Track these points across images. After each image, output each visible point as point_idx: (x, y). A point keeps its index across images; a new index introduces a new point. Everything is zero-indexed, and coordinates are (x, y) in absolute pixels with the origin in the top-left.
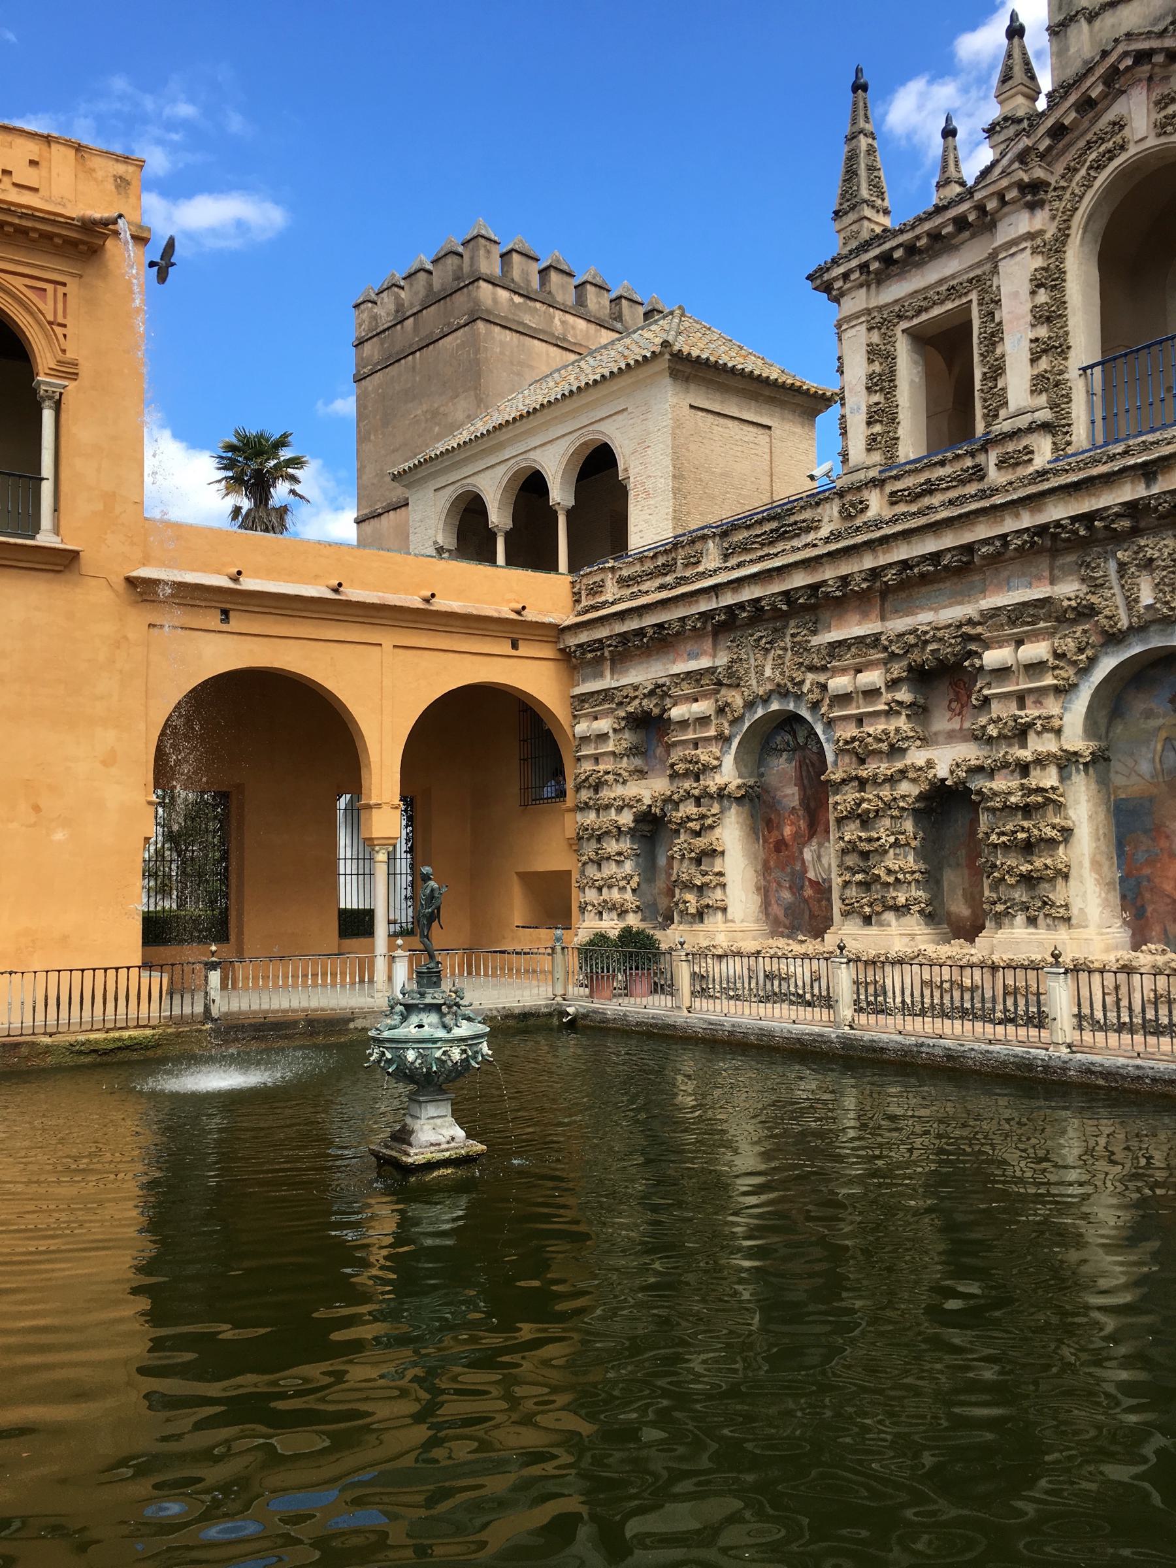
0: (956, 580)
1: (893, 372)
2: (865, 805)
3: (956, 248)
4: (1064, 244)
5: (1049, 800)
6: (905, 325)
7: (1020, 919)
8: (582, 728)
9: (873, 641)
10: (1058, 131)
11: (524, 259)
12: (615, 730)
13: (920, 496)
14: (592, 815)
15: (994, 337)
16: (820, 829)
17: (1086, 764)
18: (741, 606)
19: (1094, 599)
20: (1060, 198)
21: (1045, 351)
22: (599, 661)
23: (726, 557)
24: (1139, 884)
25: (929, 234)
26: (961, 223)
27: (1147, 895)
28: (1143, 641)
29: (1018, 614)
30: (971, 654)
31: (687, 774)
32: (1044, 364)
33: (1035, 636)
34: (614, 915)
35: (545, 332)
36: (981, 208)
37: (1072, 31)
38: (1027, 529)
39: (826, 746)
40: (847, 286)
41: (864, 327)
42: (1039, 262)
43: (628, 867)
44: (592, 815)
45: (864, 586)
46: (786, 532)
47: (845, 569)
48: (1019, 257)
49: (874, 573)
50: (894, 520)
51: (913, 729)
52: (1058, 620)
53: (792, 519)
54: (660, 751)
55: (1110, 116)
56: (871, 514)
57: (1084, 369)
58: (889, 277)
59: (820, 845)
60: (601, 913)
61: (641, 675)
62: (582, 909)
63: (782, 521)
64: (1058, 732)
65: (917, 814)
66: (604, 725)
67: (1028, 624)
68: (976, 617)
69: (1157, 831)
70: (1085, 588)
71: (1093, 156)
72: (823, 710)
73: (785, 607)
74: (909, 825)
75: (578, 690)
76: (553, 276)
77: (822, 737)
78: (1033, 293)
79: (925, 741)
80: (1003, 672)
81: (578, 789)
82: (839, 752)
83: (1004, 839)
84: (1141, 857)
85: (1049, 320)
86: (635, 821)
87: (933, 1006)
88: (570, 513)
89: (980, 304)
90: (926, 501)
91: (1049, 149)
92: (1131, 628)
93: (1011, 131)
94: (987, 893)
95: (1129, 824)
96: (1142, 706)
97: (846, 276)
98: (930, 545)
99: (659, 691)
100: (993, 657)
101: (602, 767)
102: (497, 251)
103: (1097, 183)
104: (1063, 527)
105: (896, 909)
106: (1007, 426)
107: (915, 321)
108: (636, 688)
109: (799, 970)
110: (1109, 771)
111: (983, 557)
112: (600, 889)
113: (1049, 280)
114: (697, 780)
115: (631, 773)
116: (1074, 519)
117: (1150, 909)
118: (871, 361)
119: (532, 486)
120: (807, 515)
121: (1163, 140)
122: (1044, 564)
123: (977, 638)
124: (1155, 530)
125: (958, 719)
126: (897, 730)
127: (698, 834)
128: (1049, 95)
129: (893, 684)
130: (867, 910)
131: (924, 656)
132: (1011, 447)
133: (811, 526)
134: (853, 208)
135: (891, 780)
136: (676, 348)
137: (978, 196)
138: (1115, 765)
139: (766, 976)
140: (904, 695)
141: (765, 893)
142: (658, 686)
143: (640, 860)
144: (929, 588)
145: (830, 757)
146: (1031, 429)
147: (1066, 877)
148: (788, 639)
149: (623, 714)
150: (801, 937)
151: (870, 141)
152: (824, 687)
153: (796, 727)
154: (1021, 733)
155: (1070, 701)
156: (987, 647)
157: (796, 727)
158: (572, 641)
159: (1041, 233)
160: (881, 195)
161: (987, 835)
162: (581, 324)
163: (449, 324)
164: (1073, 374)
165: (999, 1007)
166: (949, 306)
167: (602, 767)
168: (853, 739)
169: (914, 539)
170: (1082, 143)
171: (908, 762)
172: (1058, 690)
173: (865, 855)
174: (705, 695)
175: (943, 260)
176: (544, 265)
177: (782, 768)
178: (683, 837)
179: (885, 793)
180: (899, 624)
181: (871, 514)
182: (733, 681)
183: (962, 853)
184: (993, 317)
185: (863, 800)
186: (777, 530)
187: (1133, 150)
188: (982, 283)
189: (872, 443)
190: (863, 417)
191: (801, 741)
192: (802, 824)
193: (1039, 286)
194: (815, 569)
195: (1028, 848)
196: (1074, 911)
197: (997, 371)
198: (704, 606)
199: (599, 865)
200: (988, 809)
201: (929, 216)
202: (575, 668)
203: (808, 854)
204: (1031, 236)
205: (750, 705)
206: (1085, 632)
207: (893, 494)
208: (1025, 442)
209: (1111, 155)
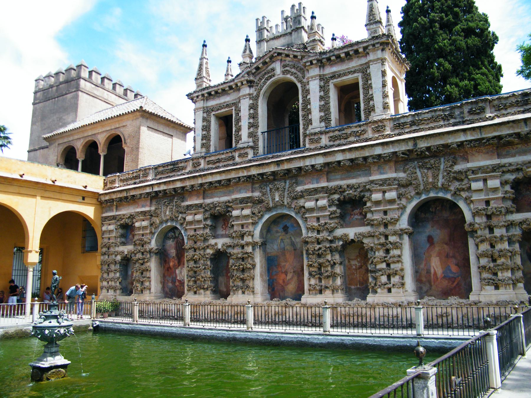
0: (225, 189)
1: (210, 126)
2: (196, 256)
3: (229, 94)
4: (258, 98)
5: (249, 256)
7: (240, 291)
8: (104, 228)
9: (200, 206)
10: (257, 68)
11: (96, 74)
12: (116, 229)
13: (216, 163)
14: (107, 257)
15: (239, 120)
16: (182, 263)
17: (260, 246)
18: (160, 191)
19: (263, 198)
20: (257, 86)
21: (252, 126)
22: (112, 206)
23: (156, 175)
24: (273, 281)
25: (222, 89)
26: (231, 88)
27: (275, 284)
28: (276, 211)
29: (243, 201)
30: (229, 211)
31: (139, 244)
32: (252, 130)
33: (247, 207)
34: (112, 291)
35: (101, 97)
36: (237, 85)
37: (262, 43)
38: (246, 176)
39: (184, 237)
41: (202, 112)
42: (251, 102)
43: (118, 275)
44: (107, 257)
45: (198, 188)
47: (192, 182)
49: (202, 185)
51: (211, 233)
52: (253, 203)
53: (177, 166)
54: (131, 236)
55: (271, 67)
56: (202, 166)
57: (262, 133)
58: (210, 99)
59: (181, 269)
60: (108, 290)
61: (126, 211)
62: (102, 288)
63: (174, 166)
64: (253, 236)
65: (212, 260)
66: (112, 227)
69: (279, 265)
70: (261, 194)
71: (266, 76)
72: (184, 226)
74: (209, 263)
75: (104, 215)
76: (106, 80)
77: (183, 235)
78: (249, 110)
79: (215, 237)
80: (237, 217)
81: (102, 248)
82: (188, 239)
83: (236, 267)
84: (274, 273)
85: (253, 118)
86: (121, 259)
87: (214, 319)
88: (105, 157)
89: (235, 110)
90: (218, 164)
91: (255, 72)
92: (272, 207)
93: (246, 66)
94: (231, 284)
95: (272, 264)
96: (275, 229)
97: (197, 97)
98: (218, 178)
99: (132, 217)
100: (235, 213)
101: (111, 241)
102: (87, 70)
103: (267, 84)
104: (255, 177)
105: (204, 289)
107: (217, 112)
108: (124, 215)
109: (173, 308)
110: (266, 248)
111: (233, 183)
112: (108, 282)
113: (254, 107)
114: (143, 246)
115: (121, 243)
116: (258, 174)
117: (276, 288)
118: (203, 122)
119: (92, 146)
120: (183, 165)
121: (284, 76)
122: (250, 185)
123: (231, 207)
124: (280, 180)
125: (224, 231)
126: (206, 233)
127: (142, 264)
128: (256, 59)
129: (206, 219)
130: (195, 289)
132: (242, 152)
133: (184, 168)
134: (201, 78)
135: (204, 249)
136: (144, 109)
137: (236, 81)
138: (268, 246)
139: (163, 311)
140: (209, 222)
141: (163, 283)
142: (131, 215)
143: (122, 272)
144: (217, 191)
145: (186, 241)
146: (247, 147)
147: (253, 279)
148: (174, 203)
149: (119, 224)
150: (174, 298)
151: (206, 60)
152: (185, 219)
153: (176, 231)
154: (242, 236)
155: (256, 227)
156: (233, 209)
157: (176, 231)
158: (103, 198)
159: (252, 94)
160: (209, 76)
161: (232, 266)
162: (114, 96)
163: (69, 91)
164: (259, 133)
165: (233, 318)
166: (227, 109)
167: (111, 241)
168: (193, 236)
169: (214, 176)
170: (263, 73)
171: (209, 243)
172: (253, 224)
173: (195, 272)
174: (147, 219)
175: (226, 96)
176: (102, 76)
177: (171, 243)
178: (137, 265)
179: (202, 252)
180: (208, 201)
181: (202, 166)
182: (156, 215)
183: (224, 272)
185: (195, 255)
186: (172, 169)
187: (276, 77)
188: (236, 104)
189: (203, 145)
191: (177, 235)
192: (176, 262)
194: (184, 182)
195: (243, 270)
196: (255, 289)
197: (239, 129)
198: (148, 190)
199: (108, 274)
200: (232, 258)
201: (222, 84)
202: (103, 207)
203: (178, 272)
204: (249, 94)
205: (161, 223)
207: (208, 161)
208: (246, 151)
209: (271, 77)
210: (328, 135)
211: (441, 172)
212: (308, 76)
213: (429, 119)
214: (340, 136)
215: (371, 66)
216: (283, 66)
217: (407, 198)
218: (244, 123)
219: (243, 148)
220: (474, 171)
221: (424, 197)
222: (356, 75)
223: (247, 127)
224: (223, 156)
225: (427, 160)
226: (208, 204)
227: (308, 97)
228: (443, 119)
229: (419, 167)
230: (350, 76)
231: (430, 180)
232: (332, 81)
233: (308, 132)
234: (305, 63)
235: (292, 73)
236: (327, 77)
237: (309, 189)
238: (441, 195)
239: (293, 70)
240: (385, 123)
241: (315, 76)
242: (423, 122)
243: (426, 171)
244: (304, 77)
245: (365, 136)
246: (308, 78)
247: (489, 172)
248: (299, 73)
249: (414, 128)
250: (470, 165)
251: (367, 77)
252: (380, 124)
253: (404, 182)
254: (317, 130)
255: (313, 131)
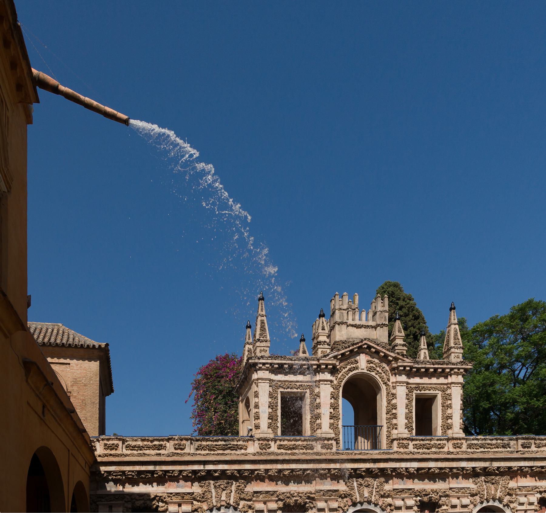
6: (282, 390)
18: (215, 471)
32: (332, 421)
40: (263, 367)
42: (332, 390)
46: (232, 447)
48: (327, 386)
50: (282, 454)
67: (330, 496)
68: (313, 492)
70: (347, 489)
71: (349, 367)
73: (238, 475)
78: (331, 399)
85: (334, 409)
89: (311, 394)
92: (360, 502)
106: (324, 436)
107: (286, 390)
113: (334, 396)
123: (313, 499)
131: (292, 501)
164: (340, 426)
184: (316, 400)
186: (227, 445)
187: (360, 371)
190: (266, 415)
193: (333, 397)
204: (331, 381)
206: (347, 501)
209: (355, 369)
210: (414, 442)
211: (500, 486)
212: (394, 381)
213: (494, 445)
214: (424, 445)
215: (452, 388)
216: (368, 361)
217: (475, 506)
218: (325, 411)
219: (329, 439)
220: (519, 488)
221: (485, 504)
222: (437, 392)
223: (329, 418)
224: (299, 443)
225: (493, 477)
226: (283, 493)
227: (394, 401)
228: (504, 447)
229: (485, 481)
230: (432, 392)
231: (493, 493)
232: (415, 392)
233: (394, 437)
234: (398, 368)
235: (378, 371)
236: (412, 386)
237: (397, 489)
238: (497, 504)
239: (378, 369)
240: (462, 441)
241: (403, 382)
242: (489, 446)
243: (490, 485)
244: (389, 380)
245: (446, 449)
246: (396, 382)
247: (529, 491)
248: (383, 374)
249: (482, 450)
250: (520, 484)
251: (447, 397)
252: (459, 441)
253: (474, 492)
254: (405, 436)
255: (400, 436)
